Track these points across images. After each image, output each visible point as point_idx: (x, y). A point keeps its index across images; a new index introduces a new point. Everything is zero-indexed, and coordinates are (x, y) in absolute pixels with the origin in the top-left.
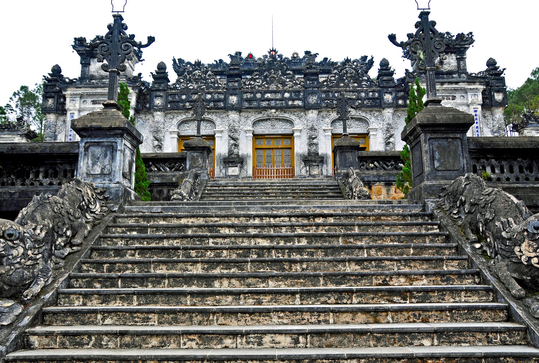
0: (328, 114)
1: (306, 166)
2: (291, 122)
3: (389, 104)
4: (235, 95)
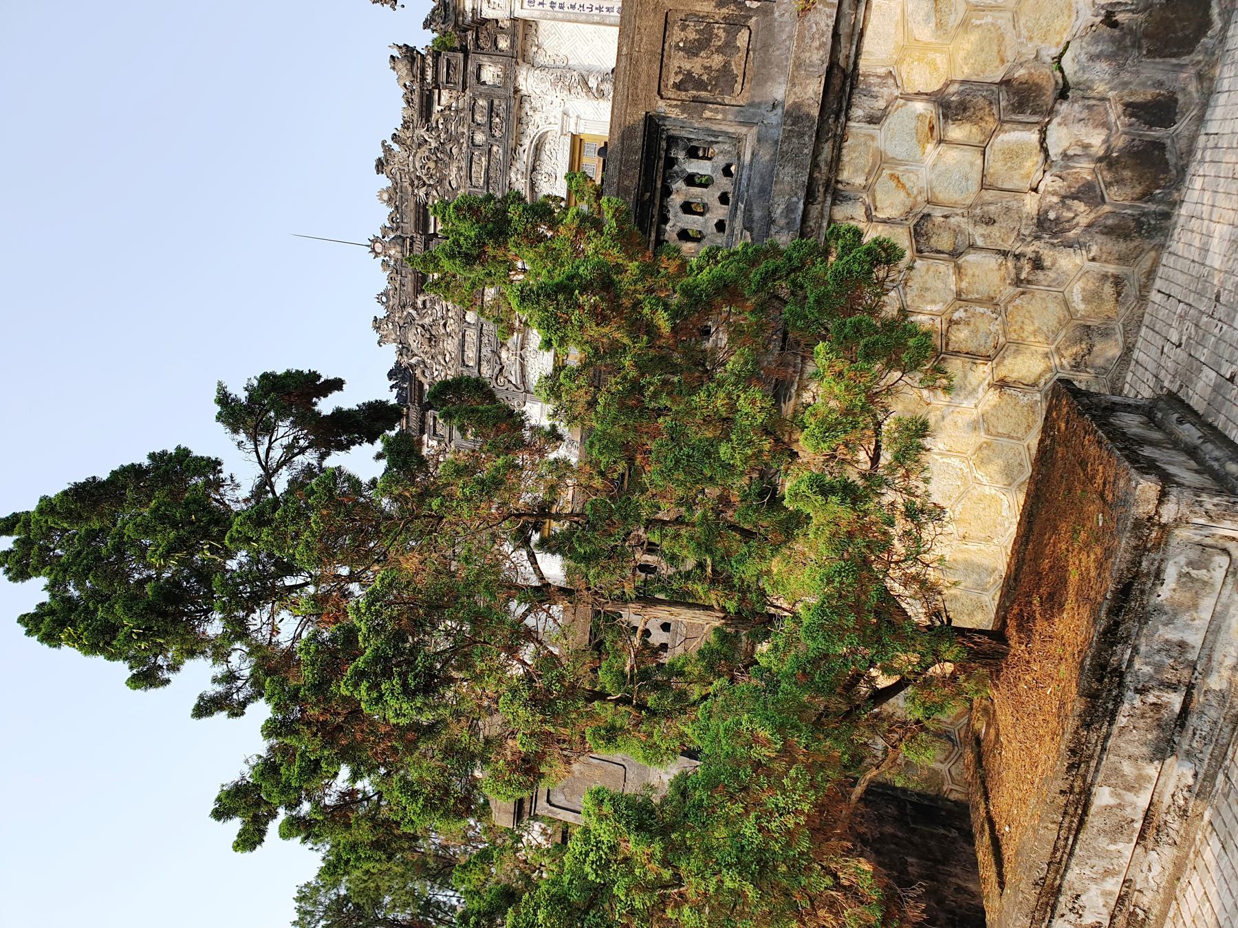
3: (506, 76)
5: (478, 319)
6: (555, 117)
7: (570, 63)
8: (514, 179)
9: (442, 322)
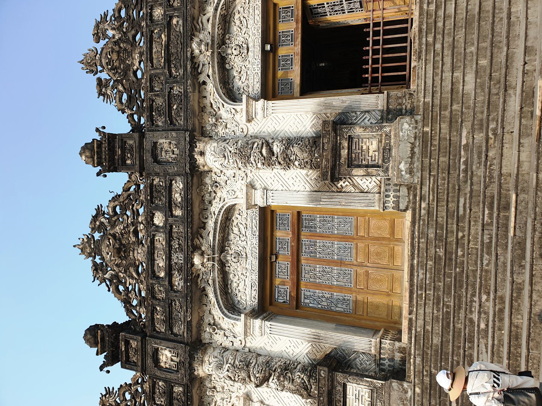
0: (209, 109)
1: (351, 176)
2: (229, 212)
4: (156, 353)
5: (166, 220)
8: (197, 52)
9: (132, 229)
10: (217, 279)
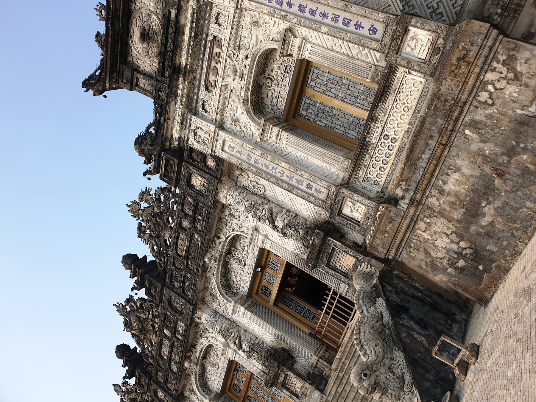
0: (210, 290)
6: (248, 228)
7: (267, 193)
10: (198, 372)
